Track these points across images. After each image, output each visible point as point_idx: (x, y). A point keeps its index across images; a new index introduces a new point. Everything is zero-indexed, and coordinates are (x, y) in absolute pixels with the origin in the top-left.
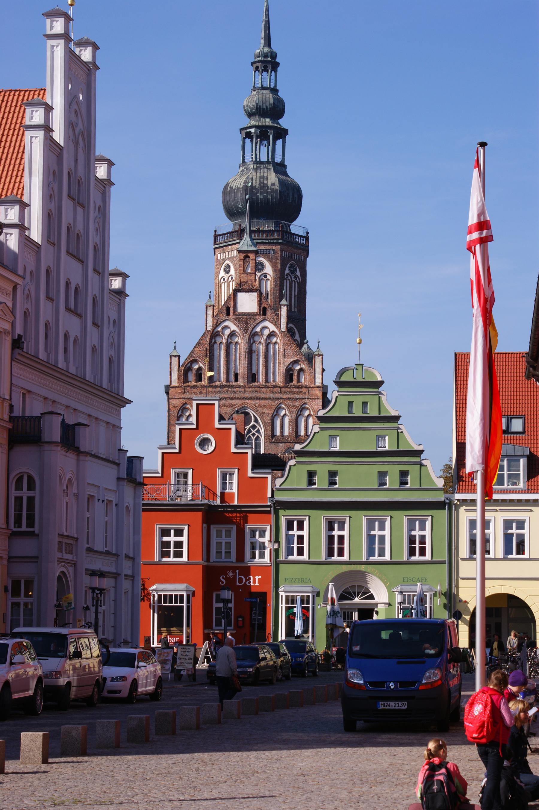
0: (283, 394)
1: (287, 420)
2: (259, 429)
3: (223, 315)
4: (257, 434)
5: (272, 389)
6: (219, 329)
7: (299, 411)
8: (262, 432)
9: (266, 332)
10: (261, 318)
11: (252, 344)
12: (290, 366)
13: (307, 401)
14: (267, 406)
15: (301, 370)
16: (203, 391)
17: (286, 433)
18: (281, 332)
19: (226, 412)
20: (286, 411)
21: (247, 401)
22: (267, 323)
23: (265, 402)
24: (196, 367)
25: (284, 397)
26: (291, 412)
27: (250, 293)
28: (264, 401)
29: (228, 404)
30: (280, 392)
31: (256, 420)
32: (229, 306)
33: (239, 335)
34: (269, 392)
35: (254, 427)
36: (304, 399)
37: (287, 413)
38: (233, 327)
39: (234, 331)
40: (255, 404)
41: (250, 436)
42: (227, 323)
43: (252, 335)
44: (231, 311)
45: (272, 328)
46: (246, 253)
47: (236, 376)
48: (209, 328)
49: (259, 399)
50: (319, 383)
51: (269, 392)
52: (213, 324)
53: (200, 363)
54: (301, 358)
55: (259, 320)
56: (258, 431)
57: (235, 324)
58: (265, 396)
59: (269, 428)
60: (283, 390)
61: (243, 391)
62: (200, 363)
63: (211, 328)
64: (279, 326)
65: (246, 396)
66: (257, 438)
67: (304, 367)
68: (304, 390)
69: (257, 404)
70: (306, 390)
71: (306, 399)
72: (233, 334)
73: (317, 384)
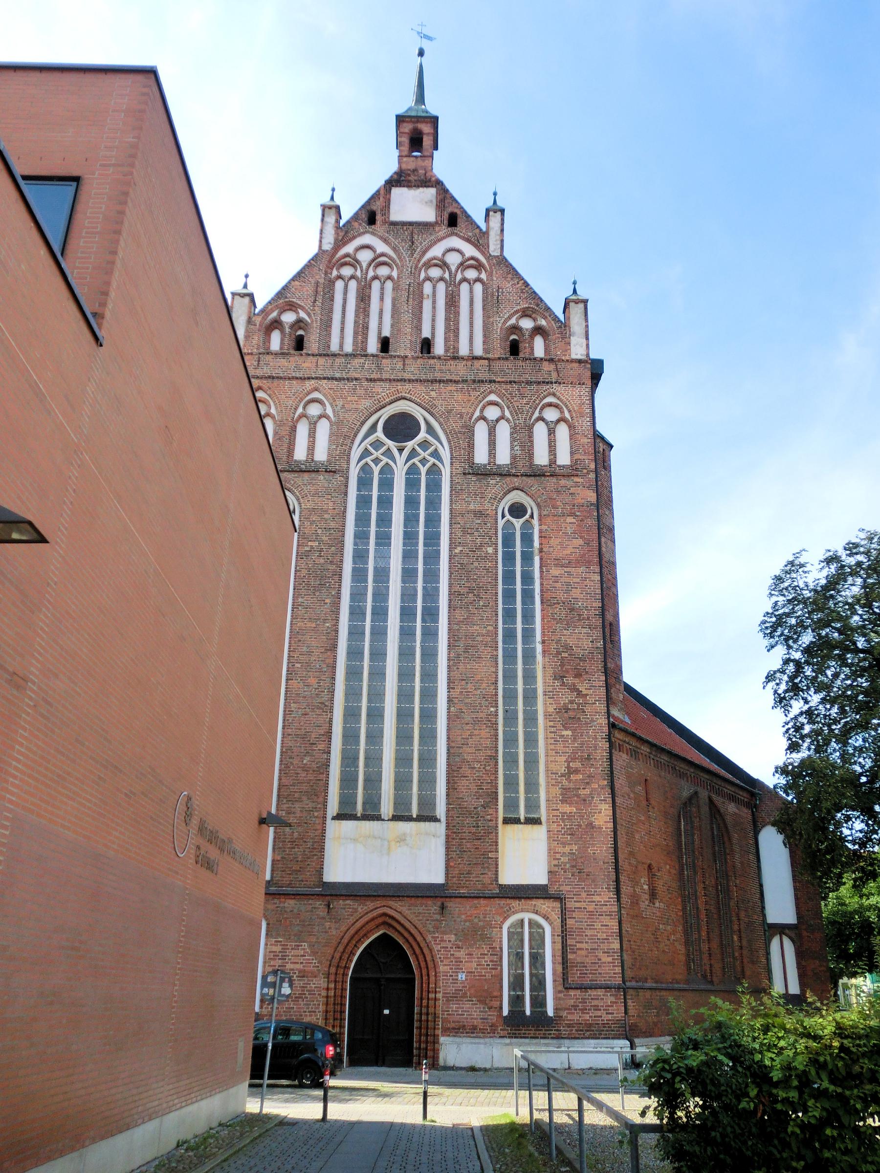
0: (495, 374)
1: (504, 431)
2: (436, 450)
3: (360, 224)
4: (432, 460)
5: (469, 363)
6: (349, 248)
7: (536, 409)
8: (445, 454)
9: (453, 260)
10: (444, 230)
11: (424, 281)
12: (513, 321)
13: (556, 388)
14: (459, 396)
15: (538, 330)
16: (303, 365)
17: (503, 457)
18: (489, 257)
19: (357, 409)
20: (503, 411)
21: (408, 386)
23: (454, 388)
24: (289, 318)
25: (499, 379)
26: (515, 412)
27: (421, 189)
28: (452, 387)
29: (362, 392)
30: (489, 370)
31: (430, 430)
32: (374, 208)
33: (394, 262)
34: (460, 370)
35: (424, 445)
36: (548, 383)
37: (507, 414)
38: (381, 247)
39: (383, 255)
40: (427, 394)
42: (367, 239)
43: (425, 264)
44: (379, 217)
45: (470, 250)
47: (385, 344)
48: (327, 247)
49: (440, 381)
50: (582, 355)
52: (336, 240)
53: (300, 311)
54: (538, 305)
55: (441, 234)
56: (436, 454)
57: (385, 241)
58: (455, 378)
59: (463, 444)
60: (497, 365)
61: (400, 365)
62: (300, 311)
63: (331, 246)
65: (407, 376)
66: (434, 471)
67: (543, 323)
68: (546, 367)
69: (433, 394)
70: (552, 367)
71: (552, 383)
72: (378, 261)
73: (574, 356)
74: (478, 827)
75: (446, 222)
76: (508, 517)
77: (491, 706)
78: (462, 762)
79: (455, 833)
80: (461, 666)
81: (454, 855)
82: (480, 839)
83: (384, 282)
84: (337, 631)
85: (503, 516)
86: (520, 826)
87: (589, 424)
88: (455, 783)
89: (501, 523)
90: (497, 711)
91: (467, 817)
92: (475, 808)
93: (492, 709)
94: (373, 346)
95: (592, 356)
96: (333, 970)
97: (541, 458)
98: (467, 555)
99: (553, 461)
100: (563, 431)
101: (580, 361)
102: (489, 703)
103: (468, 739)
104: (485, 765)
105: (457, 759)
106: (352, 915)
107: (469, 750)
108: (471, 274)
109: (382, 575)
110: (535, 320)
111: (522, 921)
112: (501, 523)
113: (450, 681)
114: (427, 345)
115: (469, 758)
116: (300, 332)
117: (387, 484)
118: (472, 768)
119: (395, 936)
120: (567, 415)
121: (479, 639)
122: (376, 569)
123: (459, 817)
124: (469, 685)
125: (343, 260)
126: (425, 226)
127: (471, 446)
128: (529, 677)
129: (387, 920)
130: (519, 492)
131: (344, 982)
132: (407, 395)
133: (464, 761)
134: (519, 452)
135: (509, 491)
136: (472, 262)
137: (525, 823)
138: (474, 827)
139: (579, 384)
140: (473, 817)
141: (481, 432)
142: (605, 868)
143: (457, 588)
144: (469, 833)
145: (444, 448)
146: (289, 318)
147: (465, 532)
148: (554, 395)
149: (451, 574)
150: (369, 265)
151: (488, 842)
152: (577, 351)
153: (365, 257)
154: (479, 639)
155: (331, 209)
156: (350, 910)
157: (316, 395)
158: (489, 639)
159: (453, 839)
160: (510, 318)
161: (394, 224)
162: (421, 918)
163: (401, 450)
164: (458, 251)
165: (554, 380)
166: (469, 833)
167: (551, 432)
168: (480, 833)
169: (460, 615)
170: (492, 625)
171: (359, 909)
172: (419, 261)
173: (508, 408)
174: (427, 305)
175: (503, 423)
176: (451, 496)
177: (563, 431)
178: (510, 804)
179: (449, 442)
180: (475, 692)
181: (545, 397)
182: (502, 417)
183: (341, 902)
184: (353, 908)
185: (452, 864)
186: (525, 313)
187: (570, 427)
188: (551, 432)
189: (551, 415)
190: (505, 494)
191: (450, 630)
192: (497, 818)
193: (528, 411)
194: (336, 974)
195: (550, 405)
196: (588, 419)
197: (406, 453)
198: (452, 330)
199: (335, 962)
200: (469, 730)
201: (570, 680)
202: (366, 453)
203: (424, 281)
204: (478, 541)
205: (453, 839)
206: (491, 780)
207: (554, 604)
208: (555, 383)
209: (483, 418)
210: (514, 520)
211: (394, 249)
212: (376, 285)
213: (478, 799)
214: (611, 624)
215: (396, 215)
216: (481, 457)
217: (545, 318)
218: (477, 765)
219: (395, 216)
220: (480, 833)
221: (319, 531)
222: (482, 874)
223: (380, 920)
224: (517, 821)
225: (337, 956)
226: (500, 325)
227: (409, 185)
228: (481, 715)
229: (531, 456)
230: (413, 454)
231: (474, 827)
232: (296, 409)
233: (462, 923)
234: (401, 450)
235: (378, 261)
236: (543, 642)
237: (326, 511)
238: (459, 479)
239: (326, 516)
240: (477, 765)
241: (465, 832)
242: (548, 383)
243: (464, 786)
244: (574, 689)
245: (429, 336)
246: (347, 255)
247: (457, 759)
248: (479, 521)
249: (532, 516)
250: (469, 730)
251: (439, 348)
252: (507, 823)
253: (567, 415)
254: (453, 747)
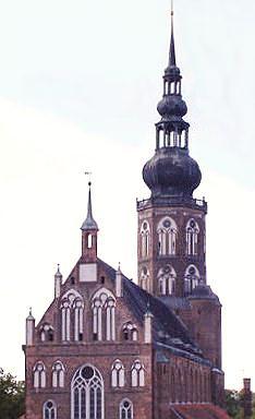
1: (122, 373)
6: (65, 296)
15: (134, 329)
17: (122, 384)
22: (104, 290)
24: (47, 328)
31: (97, 374)
34: (106, 350)
35: (95, 379)
38: (78, 295)
42: (72, 291)
45: (110, 294)
47: (80, 335)
51: (106, 350)
64: (114, 294)
66: (99, 389)
94: (77, 338)
97: (134, 384)
100: (142, 372)
108: (111, 303)
114: (96, 336)
117: (84, 395)
146: (47, 328)
153: (72, 298)
155: (59, 276)
161: (84, 283)
177: (142, 372)
202: (76, 384)
215: (82, 279)
216: (114, 384)
219: (82, 279)
227: (85, 263)
230: (92, 383)
251: (100, 338)
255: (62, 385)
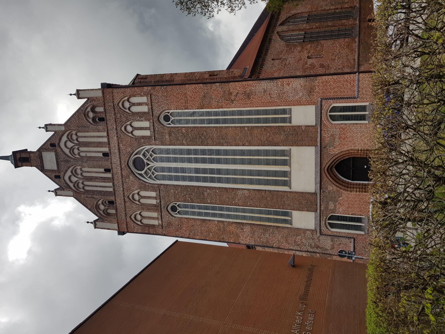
1: (136, 124)
2: (146, 151)
6: (71, 185)
7: (125, 111)
8: (148, 147)
9: (70, 145)
11: (80, 156)
12: (91, 120)
14: (124, 142)
15: (93, 110)
17: (146, 124)
24: (102, 207)
26: (128, 120)
33: (74, 168)
35: (144, 155)
37: (129, 123)
38: (69, 173)
39: (72, 172)
40: (125, 155)
41: (153, 159)
42: (66, 178)
44: (57, 174)
45: (64, 138)
46: (17, 161)
47: (107, 170)
67: (89, 109)
74: (292, 134)
75: (55, 148)
76: (170, 122)
77: (245, 129)
78: (267, 140)
79: (295, 143)
80: (230, 141)
81: (304, 143)
82: (297, 133)
83: (83, 171)
84: (220, 188)
85: (170, 124)
86: (292, 116)
87: (128, 89)
88: (275, 143)
89: (172, 125)
90: (247, 127)
91: (289, 138)
92: (285, 135)
93: (246, 129)
94: (109, 175)
95: (100, 87)
96: (349, 189)
97: (145, 109)
98: (187, 139)
99: (146, 104)
101: (103, 93)
102: (244, 130)
103: (258, 138)
104: (268, 131)
105: (266, 142)
106: (328, 182)
107: (262, 137)
109: (197, 171)
110: (88, 112)
111: (330, 115)
112: (172, 125)
113: (236, 145)
114: (105, 155)
115: (265, 137)
116: (107, 202)
118: (269, 136)
119: (334, 166)
120: (126, 98)
121: (219, 134)
122: (195, 173)
123: (289, 142)
124: (237, 138)
125: (76, 187)
126: (57, 156)
127: (143, 137)
128: (233, 113)
129: (330, 169)
130: (160, 118)
131: (354, 184)
132: (126, 163)
133: (267, 140)
134: (143, 118)
135: (160, 122)
136: (69, 137)
137: (291, 115)
138: (292, 136)
139: (112, 93)
140: (289, 136)
141: (137, 133)
142: (309, 81)
143: (200, 142)
144: (295, 137)
145: (145, 148)
147: (178, 140)
148: (119, 103)
149: (194, 145)
150: (77, 177)
151: (299, 130)
152: (100, 94)
154: (219, 134)
155: (56, 192)
156: (326, 183)
157: (131, 197)
158: (219, 130)
159: (297, 143)
160: (89, 122)
162: (329, 156)
163: (148, 164)
164: (65, 143)
165: (112, 104)
166: (295, 137)
167: (134, 104)
168: (295, 133)
169: (210, 141)
170: (213, 129)
171: (325, 179)
172: (72, 158)
173: (126, 123)
174: (89, 155)
175: (133, 124)
176: (164, 145)
177: (134, 100)
178: (284, 120)
179: (143, 146)
180: (240, 135)
181: (120, 108)
182: (131, 125)
183: (323, 186)
184: (325, 181)
185: (307, 144)
186: (86, 115)
187: (131, 97)
188: (134, 104)
189: (127, 105)
190: (161, 124)
191: (216, 145)
192: (289, 126)
193: (127, 115)
194: (351, 188)
195: (123, 105)
196: (126, 89)
197: (149, 162)
198: (99, 144)
199: (346, 188)
200: (254, 138)
201: (233, 98)
203: (80, 156)
204: (181, 135)
205: (297, 143)
206: (274, 129)
207: (203, 104)
208: (113, 103)
209: (132, 132)
210: (171, 120)
211: (69, 168)
212: (85, 174)
213: (281, 134)
214: (210, 76)
216: (147, 133)
217: (87, 108)
218: (268, 134)
219: (55, 168)
220: (295, 133)
221: (183, 195)
222: (311, 132)
223: (330, 171)
224: (290, 118)
225: (343, 188)
226: (93, 126)
228: (248, 133)
229: (145, 113)
231: (292, 136)
232: (137, 204)
233: (331, 140)
234: (148, 164)
235: (74, 173)
236: (219, 108)
237: (175, 192)
238: (157, 142)
239: (176, 192)
240: (268, 134)
241: (295, 139)
242: (114, 107)
243: (277, 140)
244: (236, 96)
245: (102, 153)
246: (74, 186)
247: (266, 142)
248: (173, 134)
249: (169, 113)
250: (254, 138)
251: (106, 150)
252: (291, 122)
253: (126, 98)
254: (262, 144)
255: (153, 194)
